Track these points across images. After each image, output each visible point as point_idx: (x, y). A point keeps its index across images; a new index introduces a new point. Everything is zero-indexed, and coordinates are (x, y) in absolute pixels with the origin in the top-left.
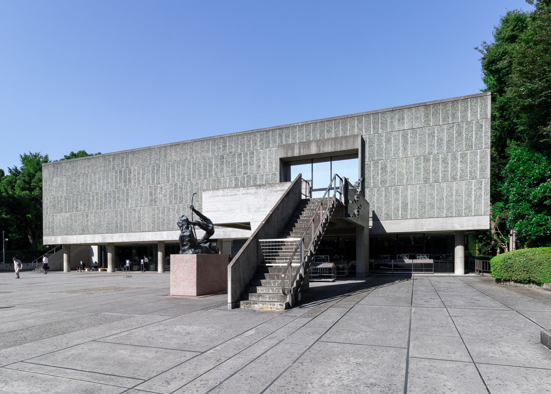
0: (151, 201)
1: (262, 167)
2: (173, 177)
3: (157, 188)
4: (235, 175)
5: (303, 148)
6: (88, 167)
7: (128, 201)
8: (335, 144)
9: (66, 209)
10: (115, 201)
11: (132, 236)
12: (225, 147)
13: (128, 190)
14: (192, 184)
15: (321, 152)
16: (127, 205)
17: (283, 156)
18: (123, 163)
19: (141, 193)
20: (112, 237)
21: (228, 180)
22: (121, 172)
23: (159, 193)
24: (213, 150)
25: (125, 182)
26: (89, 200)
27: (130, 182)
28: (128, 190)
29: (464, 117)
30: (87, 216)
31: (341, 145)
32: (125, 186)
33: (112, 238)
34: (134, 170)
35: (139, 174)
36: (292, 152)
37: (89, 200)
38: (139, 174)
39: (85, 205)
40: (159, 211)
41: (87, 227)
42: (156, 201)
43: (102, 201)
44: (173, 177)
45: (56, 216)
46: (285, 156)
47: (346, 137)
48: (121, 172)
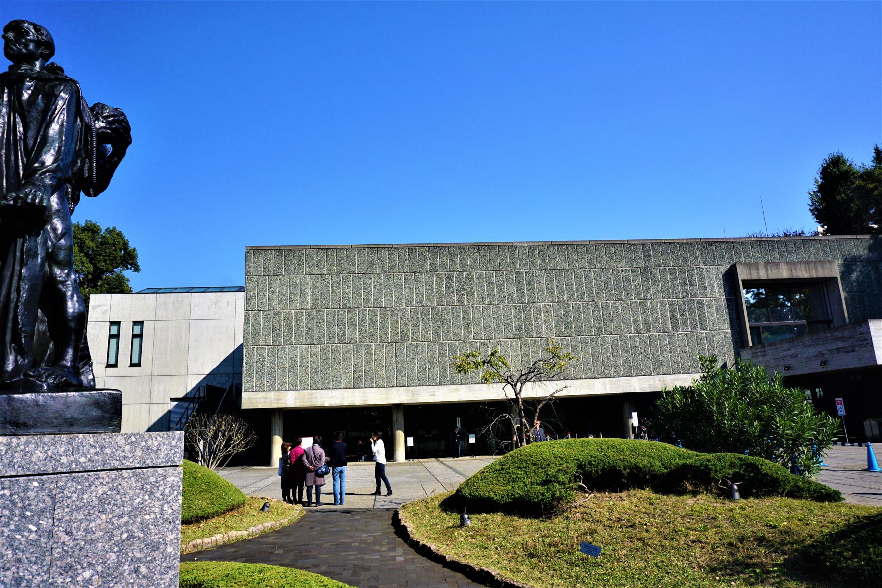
1: (708, 291)
2: (561, 291)
4: (670, 298)
5: (772, 270)
6: (372, 263)
8: (809, 269)
11: (480, 390)
13: (466, 310)
14: (597, 306)
15: (794, 277)
18: (455, 263)
20: (434, 392)
21: (658, 304)
22: (449, 278)
24: (629, 260)
25: (460, 295)
26: (373, 323)
27: (471, 293)
28: (466, 310)
30: (368, 352)
31: (816, 270)
32: (460, 302)
33: (432, 394)
34: (480, 277)
35: (489, 283)
36: (757, 274)
37: (373, 323)
38: (489, 283)
40: (537, 347)
45: (284, 350)
46: (749, 278)
48: (449, 278)
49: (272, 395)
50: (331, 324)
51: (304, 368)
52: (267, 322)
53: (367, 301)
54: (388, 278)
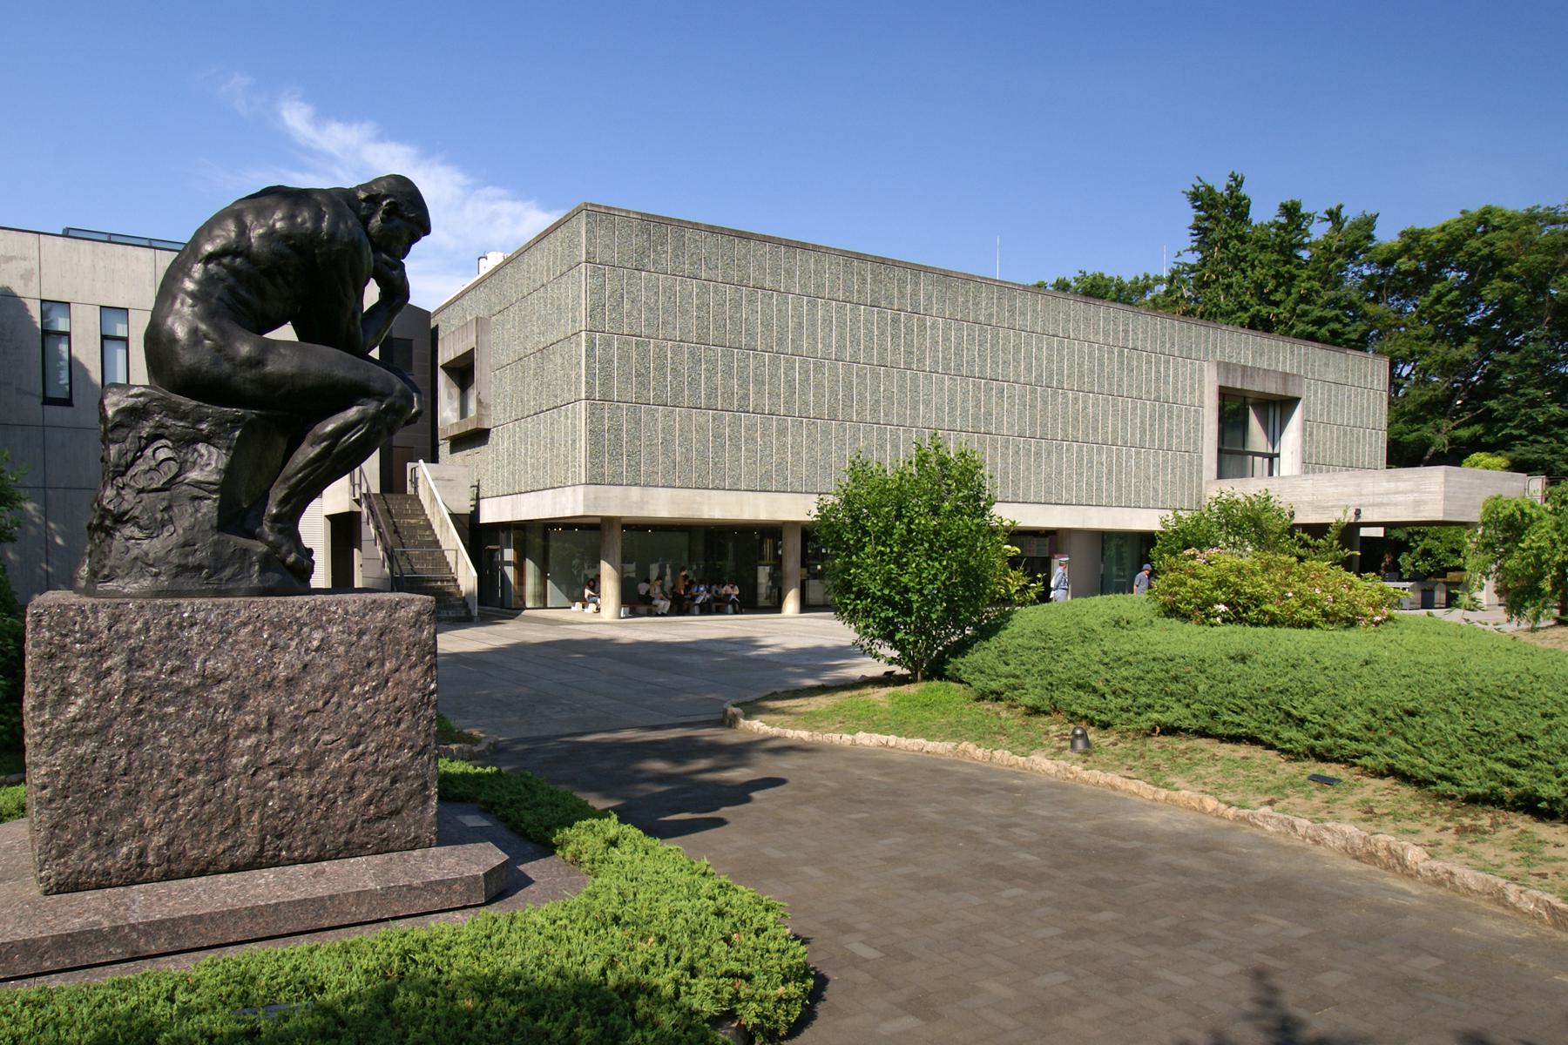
0: (976, 418)
2: (1029, 369)
3: (992, 389)
7: (915, 409)
9: (695, 393)
10: (878, 401)
12: (1126, 331)
16: (914, 417)
17: (1223, 385)
19: (952, 393)
23: (997, 403)
26: (790, 383)
29: (1372, 382)
30: (782, 432)
34: (933, 326)
35: (946, 339)
37: (790, 383)
39: (774, 395)
41: (781, 467)
42: (988, 423)
43: (834, 393)
44: (1029, 369)
45: (652, 414)
47: (1294, 375)
49: (635, 492)
50: (728, 373)
51: (684, 450)
52: (626, 358)
53: (781, 341)
54: (813, 305)
